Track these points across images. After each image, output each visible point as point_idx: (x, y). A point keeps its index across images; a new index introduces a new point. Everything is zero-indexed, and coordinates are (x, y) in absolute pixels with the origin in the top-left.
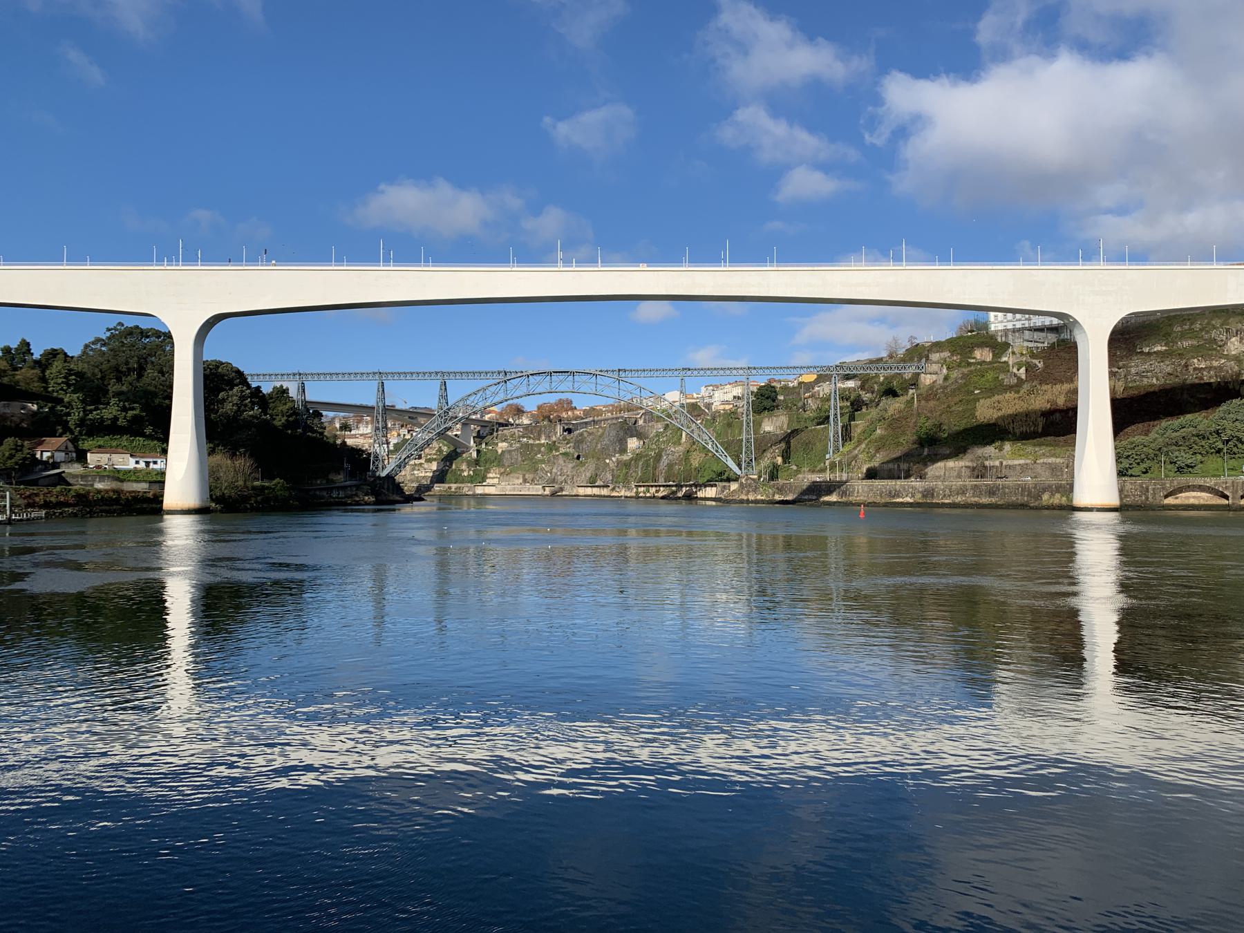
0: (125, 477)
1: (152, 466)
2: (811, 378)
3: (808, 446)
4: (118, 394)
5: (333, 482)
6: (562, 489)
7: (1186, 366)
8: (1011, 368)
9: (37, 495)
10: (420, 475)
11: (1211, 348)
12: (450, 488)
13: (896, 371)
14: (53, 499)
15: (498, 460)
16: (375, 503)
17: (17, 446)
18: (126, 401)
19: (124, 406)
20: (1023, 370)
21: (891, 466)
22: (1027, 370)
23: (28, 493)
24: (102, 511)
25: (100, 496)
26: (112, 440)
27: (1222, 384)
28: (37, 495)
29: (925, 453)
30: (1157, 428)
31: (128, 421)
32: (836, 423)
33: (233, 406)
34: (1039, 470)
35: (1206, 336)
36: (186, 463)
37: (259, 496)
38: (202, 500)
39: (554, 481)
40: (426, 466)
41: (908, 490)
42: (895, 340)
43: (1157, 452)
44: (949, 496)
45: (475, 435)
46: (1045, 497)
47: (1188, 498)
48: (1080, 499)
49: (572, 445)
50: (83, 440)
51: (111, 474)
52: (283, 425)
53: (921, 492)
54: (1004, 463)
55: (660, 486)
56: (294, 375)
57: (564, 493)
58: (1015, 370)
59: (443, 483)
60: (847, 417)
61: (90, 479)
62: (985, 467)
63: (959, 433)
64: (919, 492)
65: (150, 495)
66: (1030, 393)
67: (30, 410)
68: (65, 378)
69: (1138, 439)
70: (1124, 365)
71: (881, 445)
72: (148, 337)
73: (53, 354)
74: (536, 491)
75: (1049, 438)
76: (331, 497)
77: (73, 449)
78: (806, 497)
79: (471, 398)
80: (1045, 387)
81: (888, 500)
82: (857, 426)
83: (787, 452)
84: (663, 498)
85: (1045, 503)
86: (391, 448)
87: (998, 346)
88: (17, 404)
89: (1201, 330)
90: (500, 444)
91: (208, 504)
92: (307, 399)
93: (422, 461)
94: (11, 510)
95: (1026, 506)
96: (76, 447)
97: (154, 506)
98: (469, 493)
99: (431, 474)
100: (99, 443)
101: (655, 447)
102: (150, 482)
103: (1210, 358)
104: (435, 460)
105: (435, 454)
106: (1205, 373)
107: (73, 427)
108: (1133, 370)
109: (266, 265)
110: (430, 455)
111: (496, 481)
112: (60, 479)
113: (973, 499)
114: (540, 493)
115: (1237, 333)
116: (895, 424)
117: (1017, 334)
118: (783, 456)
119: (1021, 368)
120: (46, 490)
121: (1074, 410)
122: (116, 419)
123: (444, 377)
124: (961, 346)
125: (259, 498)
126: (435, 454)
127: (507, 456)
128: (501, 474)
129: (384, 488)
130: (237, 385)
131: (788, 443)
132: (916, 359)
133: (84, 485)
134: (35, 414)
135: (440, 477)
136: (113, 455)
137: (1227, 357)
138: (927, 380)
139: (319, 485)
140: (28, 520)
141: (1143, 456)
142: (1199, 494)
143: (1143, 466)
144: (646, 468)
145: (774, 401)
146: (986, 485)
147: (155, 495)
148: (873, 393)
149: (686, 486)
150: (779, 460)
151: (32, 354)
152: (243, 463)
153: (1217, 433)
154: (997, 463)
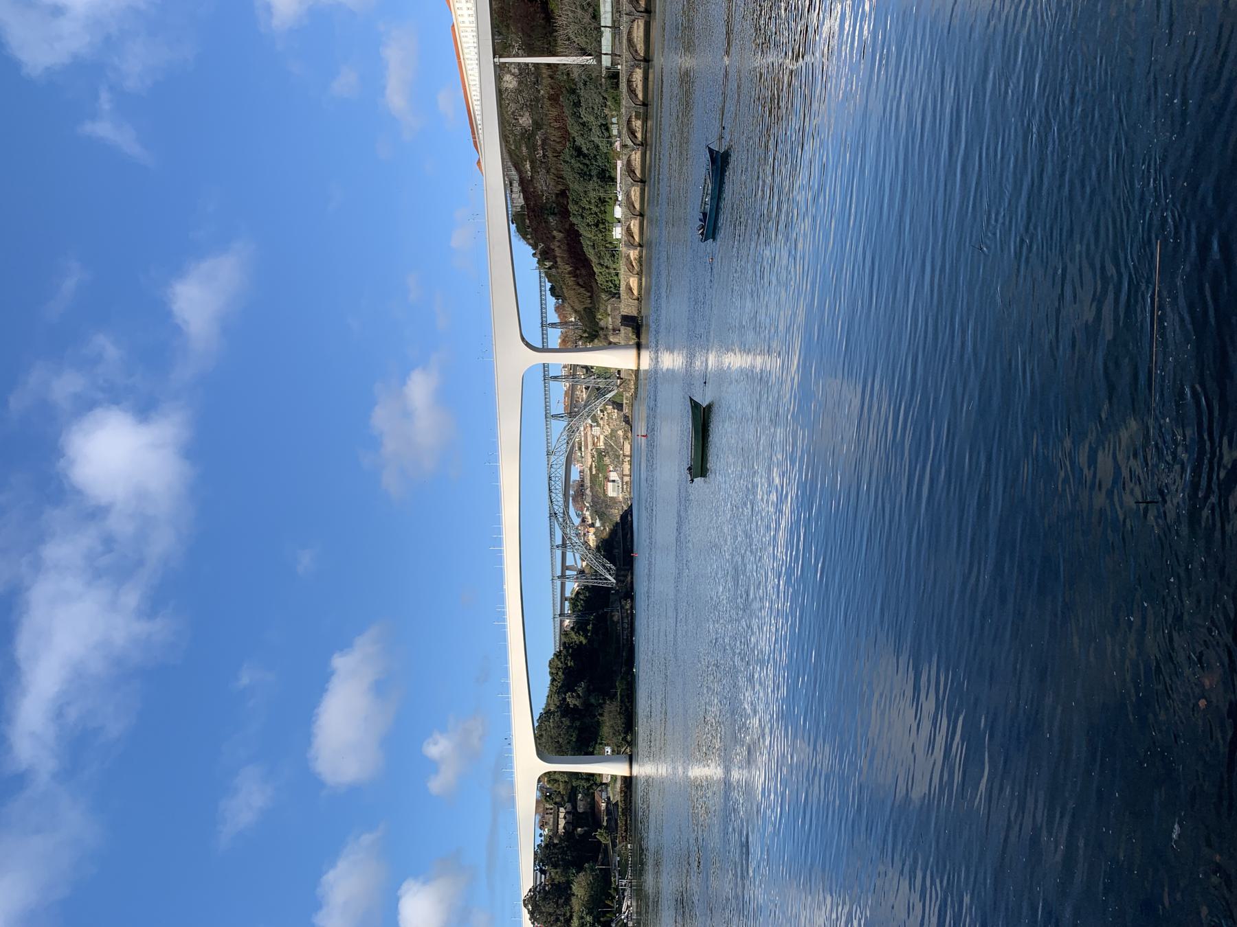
5: (618, 622)
9: (622, 834)
12: (626, 403)
28: (622, 834)
38: (626, 761)
52: (586, 637)
59: (622, 404)
70: (541, 192)
86: (595, 424)
88: (579, 803)
96: (600, 786)
99: (616, 411)
129: (624, 582)
130: (566, 698)
135: (619, 406)
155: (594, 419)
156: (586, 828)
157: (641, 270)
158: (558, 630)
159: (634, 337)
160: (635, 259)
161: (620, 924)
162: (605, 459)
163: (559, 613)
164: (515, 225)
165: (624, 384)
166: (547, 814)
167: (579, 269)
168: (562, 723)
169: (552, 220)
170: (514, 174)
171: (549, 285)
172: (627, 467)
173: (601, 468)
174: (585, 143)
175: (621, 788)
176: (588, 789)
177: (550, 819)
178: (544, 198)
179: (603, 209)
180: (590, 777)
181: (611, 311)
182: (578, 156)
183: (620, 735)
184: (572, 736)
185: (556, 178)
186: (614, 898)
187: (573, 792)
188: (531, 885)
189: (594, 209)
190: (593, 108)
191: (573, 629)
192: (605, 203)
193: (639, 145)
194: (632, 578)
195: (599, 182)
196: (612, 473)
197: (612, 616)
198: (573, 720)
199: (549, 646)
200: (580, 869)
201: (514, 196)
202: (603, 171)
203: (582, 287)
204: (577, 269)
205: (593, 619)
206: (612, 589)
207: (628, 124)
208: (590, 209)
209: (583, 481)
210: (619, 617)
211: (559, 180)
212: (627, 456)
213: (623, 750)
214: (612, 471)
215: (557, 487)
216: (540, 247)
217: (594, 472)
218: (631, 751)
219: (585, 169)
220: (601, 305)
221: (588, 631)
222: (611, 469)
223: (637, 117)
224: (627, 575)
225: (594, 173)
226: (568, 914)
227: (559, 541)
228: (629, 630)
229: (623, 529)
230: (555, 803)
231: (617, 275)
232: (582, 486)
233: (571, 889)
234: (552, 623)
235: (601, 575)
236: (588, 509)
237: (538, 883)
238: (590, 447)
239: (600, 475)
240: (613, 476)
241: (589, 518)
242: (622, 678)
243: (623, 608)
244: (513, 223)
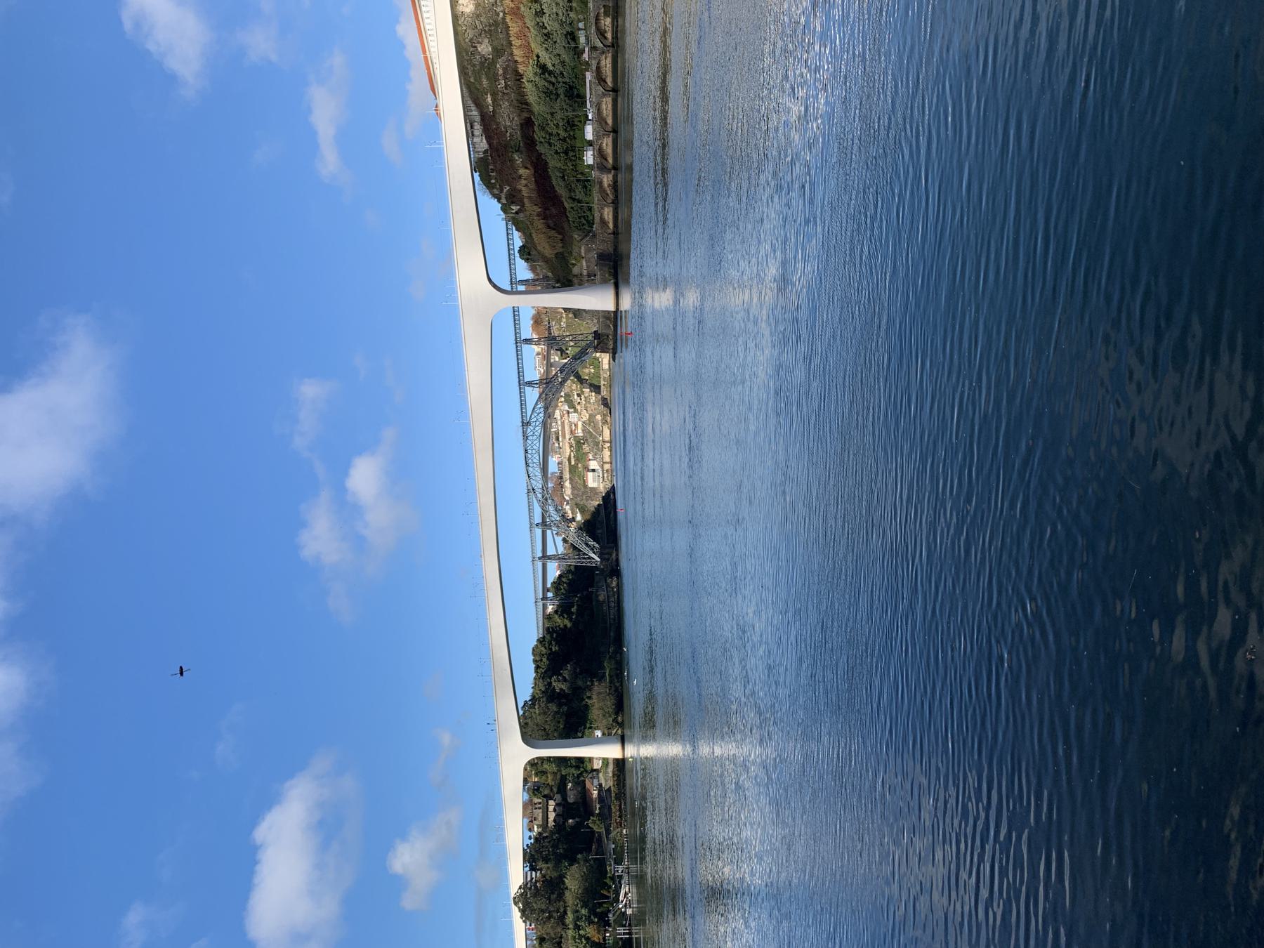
5: (604, 602)
9: (616, 820)
12: (604, 385)
28: (616, 820)
35: (478, 67)
52: (571, 620)
59: (600, 386)
70: (504, 128)
86: (572, 410)
88: (569, 793)
91: (620, 738)
93: (583, 396)
98: (608, 373)
99: (593, 394)
115: (475, 47)
117: (477, 146)
129: (608, 559)
130: (551, 683)
134: (573, 786)
135: (596, 388)
155: (571, 405)
156: (577, 819)
157: (616, 197)
158: (541, 616)
159: (612, 277)
160: (609, 185)
161: (618, 913)
162: (584, 447)
163: (541, 597)
164: (478, 173)
166: (536, 808)
167: (549, 209)
168: (548, 709)
169: (517, 158)
170: (475, 114)
171: (518, 242)
172: (607, 453)
173: (580, 457)
174: (550, 58)
175: (613, 772)
176: (579, 776)
177: (539, 814)
178: (508, 135)
179: (572, 134)
180: (580, 760)
181: (585, 254)
182: (543, 73)
183: (610, 716)
184: (559, 722)
185: (520, 105)
186: (610, 887)
187: (563, 781)
188: (520, 881)
189: (563, 134)
190: (557, 14)
191: (556, 612)
192: (575, 126)
193: (609, 46)
194: (617, 555)
195: (567, 101)
196: (591, 461)
197: (597, 596)
198: (560, 705)
199: (530, 632)
200: (573, 861)
201: (475, 140)
202: (571, 88)
203: (554, 229)
204: (546, 209)
205: (577, 601)
206: (596, 568)
207: (596, 23)
208: (558, 135)
209: (561, 473)
210: (604, 596)
211: (524, 106)
212: (608, 442)
213: (614, 731)
214: (592, 460)
215: (535, 461)
217: (573, 463)
218: (623, 732)
219: (551, 88)
220: (574, 247)
221: (572, 613)
222: (591, 457)
223: (606, 14)
224: (612, 552)
225: (561, 91)
226: (562, 910)
227: (538, 519)
228: (616, 608)
229: (606, 508)
230: (545, 796)
231: (590, 209)
232: (561, 478)
233: (564, 883)
234: (534, 607)
235: (584, 554)
236: (568, 504)
237: (529, 879)
238: (568, 436)
239: (580, 465)
240: (593, 465)
241: (570, 512)
242: (610, 657)
243: (609, 586)
244: (476, 172)
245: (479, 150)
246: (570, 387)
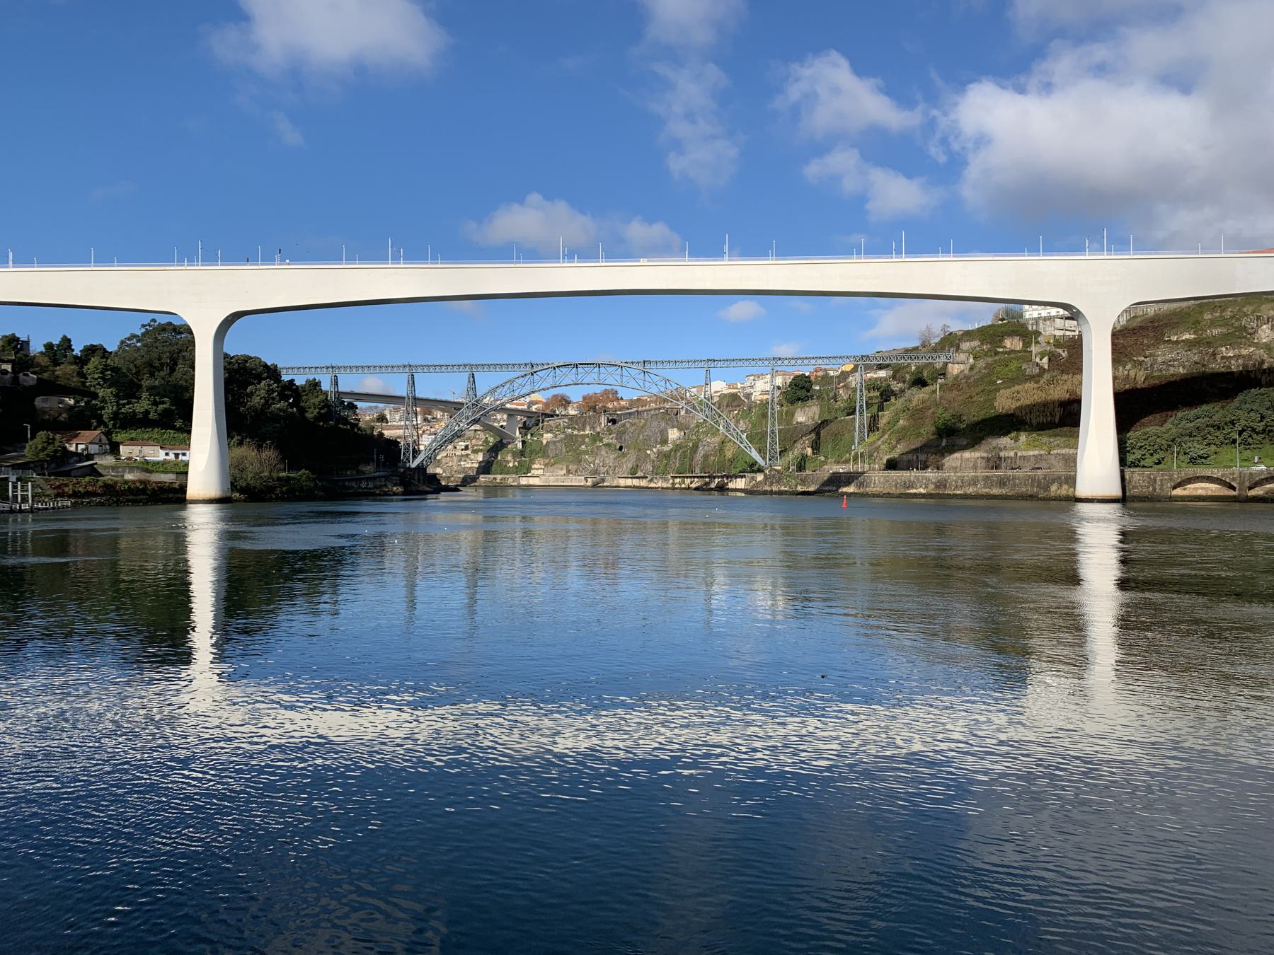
0: (154, 468)
1: (181, 457)
2: (848, 368)
3: (837, 436)
4: (150, 389)
5: (363, 473)
6: (603, 480)
7: (1214, 354)
8: (1033, 357)
9: (66, 485)
10: (467, 466)
11: (1241, 335)
12: (495, 479)
13: (930, 361)
14: (80, 489)
15: (543, 451)
16: (403, 494)
17: (49, 439)
18: (156, 395)
19: (155, 400)
20: (1045, 360)
21: (910, 457)
22: (1050, 360)
23: (57, 483)
24: (128, 501)
25: (126, 487)
26: (144, 432)
27: (1244, 373)
28: (66, 485)
29: (944, 444)
30: (1173, 418)
31: (159, 414)
32: (861, 413)
33: (261, 399)
34: (1053, 461)
36: (207, 455)
37: (284, 486)
38: (223, 491)
39: (596, 472)
40: (472, 457)
41: (922, 481)
42: (928, 329)
43: (1170, 443)
44: (961, 487)
45: (521, 425)
46: (1054, 488)
47: (1196, 489)
48: (1082, 490)
49: (614, 435)
50: (116, 433)
51: (141, 465)
52: (317, 419)
53: (935, 483)
54: (1019, 454)
55: (694, 477)
56: (327, 368)
57: (605, 484)
58: (1038, 360)
59: (489, 474)
60: (876, 407)
61: (120, 470)
62: (1000, 458)
63: (978, 423)
64: (932, 483)
65: (176, 486)
66: (1049, 383)
67: (67, 404)
68: (101, 373)
69: (1152, 429)
70: (1151, 354)
71: (902, 436)
72: (181, 333)
73: (91, 350)
74: (579, 482)
75: (1065, 429)
76: (360, 487)
77: (107, 442)
78: (827, 488)
79: (499, 390)
80: (1065, 377)
81: (903, 491)
82: (883, 415)
83: (816, 443)
84: (696, 489)
85: (1052, 494)
87: (1027, 334)
89: (1232, 317)
90: (545, 435)
91: (229, 494)
92: (340, 390)
93: (469, 452)
94: (33, 500)
95: (1036, 497)
96: (109, 440)
97: (180, 495)
99: (477, 465)
100: (131, 436)
101: (694, 437)
102: (177, 473)
103: (1239, 346)
104: (481, 450)
105: (481, 445)
106: (1233, 362)
107: (107, 420)
108: (1160, 359)
109: (280, 264)
110: (477, 446)
111: (540, 472)
112: (93, 471)
113: (984, 490)
114: (582, 484)
115: (1268, 321)
116: (916, 415)
117: (1048, 323)
118: (812, 447)
119: (1044, 357)
120: (75, 481)
121: (1079, 401)
122: (147, 412)
123: (471, 370)
124: (991, 335)
125: (284, 489)
126: (481, 445)
127: (552, 447)
128: (546, 465)
131: (818, 434)
132: (947, 348)
133: (116, 476)
134: (72, 407)
135: (485, 468)
136: (144, 448)
137: (1257, 345)
138: (954, 369)
139: (348, 476)
140: (53, 508)
141: (1156, 447)
142: (1208, 485)
143: (1156, 457)
144: (682, 458)
145: (808, 391)
146: (997, 476)
147: (180, 485)
148: (904, 382)
149: (718, 477)
150: (809, 451)
151: (73, 350)
152: (269, 454)
153: (1232, 423)
154: (1012, 454)
165: (778, 476)
178: (1141, 359)
197: (367, 462)
216: (1060, 351)
221: (326, 421)
245: (1041, 325)
246: (475, 438)
